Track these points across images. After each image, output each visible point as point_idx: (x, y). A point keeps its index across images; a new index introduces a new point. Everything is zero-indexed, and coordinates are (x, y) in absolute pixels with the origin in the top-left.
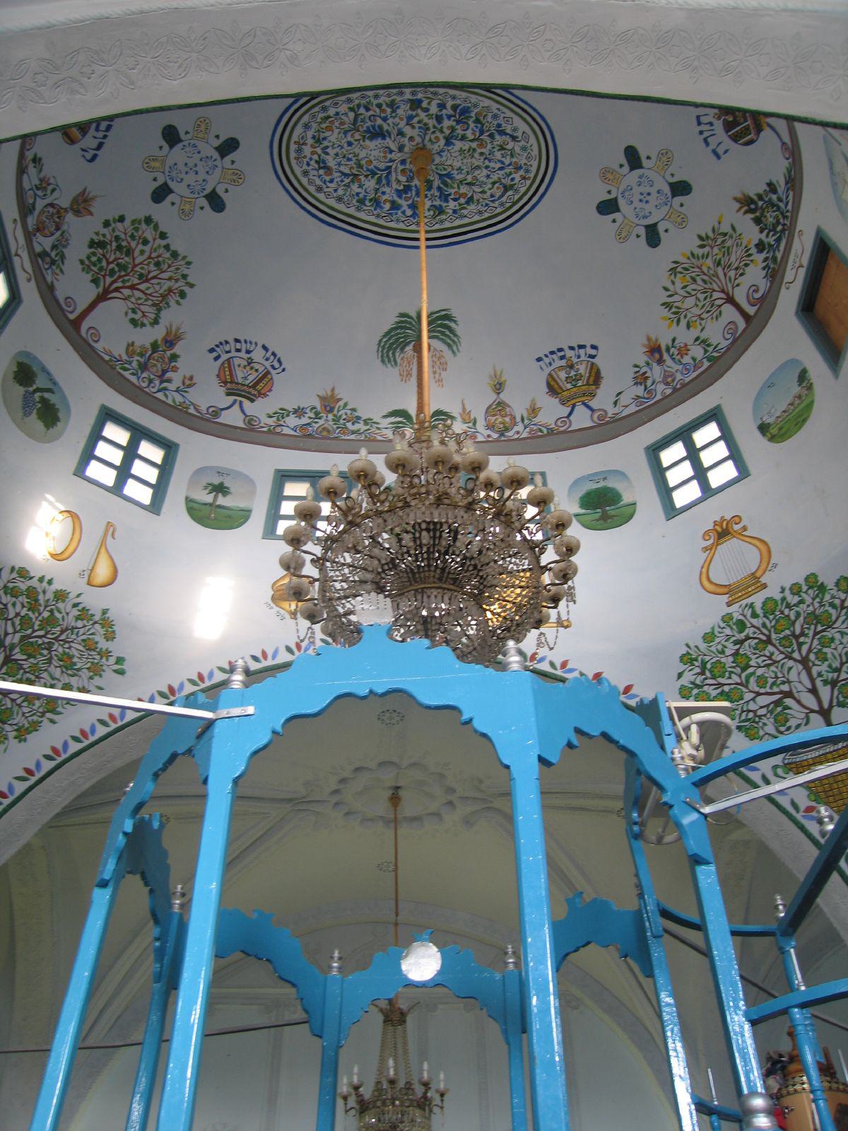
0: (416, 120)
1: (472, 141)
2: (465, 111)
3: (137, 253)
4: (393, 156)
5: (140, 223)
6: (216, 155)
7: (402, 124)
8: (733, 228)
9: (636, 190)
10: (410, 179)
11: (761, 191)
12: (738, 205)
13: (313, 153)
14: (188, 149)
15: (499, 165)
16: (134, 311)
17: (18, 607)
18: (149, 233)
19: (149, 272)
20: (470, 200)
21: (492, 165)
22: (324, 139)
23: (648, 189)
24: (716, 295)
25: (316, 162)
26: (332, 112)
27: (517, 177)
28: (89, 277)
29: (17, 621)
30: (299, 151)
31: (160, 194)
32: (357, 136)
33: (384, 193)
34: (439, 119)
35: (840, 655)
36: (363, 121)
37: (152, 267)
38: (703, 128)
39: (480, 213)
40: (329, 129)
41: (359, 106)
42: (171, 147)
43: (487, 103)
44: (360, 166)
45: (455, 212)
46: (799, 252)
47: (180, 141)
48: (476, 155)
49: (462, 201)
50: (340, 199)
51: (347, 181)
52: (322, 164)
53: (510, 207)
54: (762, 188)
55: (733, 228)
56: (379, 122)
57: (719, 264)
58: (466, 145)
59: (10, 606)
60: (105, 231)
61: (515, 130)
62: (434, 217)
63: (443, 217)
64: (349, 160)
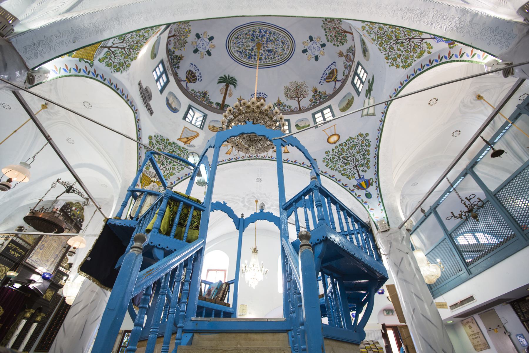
0: (261, 54)
1: (247, 49)
2: (249, 57)
3: (334, 35)
4: (266, 45)
5: (330, 41)
6: (308, 50)
7: (263, 54)
8: (181, 50)
9: (206, 45)
10: (262, 39)
11: (180, 64)
12: (182, 56)
13: (285, 46)
14: (314, 54)
15: (240, 43)
16: (340, 23)
17: (386, 46)
18: (329, 37)
19: (333, 29)
20: (246, 34)
21: (242, 43)
22: (282, 50)
23: (203, 47)
24: (178, 33)
25: (284, 44)
26: (280, 57)
27: (235, 41)
28: (346, 38)
29: (389, 43)
30: (288, 47)
31: (323, 45)
32: (274, 50)
33: (268, 35)
34: (255, 55)
35: (117, 57)
36: (273, 54)
37: (331, 30)
38: (197, 69)
39: (243, 31)
40: (281, 53)
41: (273, 59)
42: (317, 56)
43: (245, 60)
44: (274, 42)
45: (250, 31)
46: (170, 71)
47: (315, 56)
48: (246, 46)
49: (248, 34)
50: (280, 34)
51: (278, 39)
52: (283, 43)
53: (236, 33)
54: (180, 65)
55: (181, 50)
56: (269, 54)
57: (180, 40)
58: (248, 48)
59: (388, 47)
60: (339, 44)
61: (237, 53)
62: (255, 30)
63: (253, 30)
64: (276, 44)
